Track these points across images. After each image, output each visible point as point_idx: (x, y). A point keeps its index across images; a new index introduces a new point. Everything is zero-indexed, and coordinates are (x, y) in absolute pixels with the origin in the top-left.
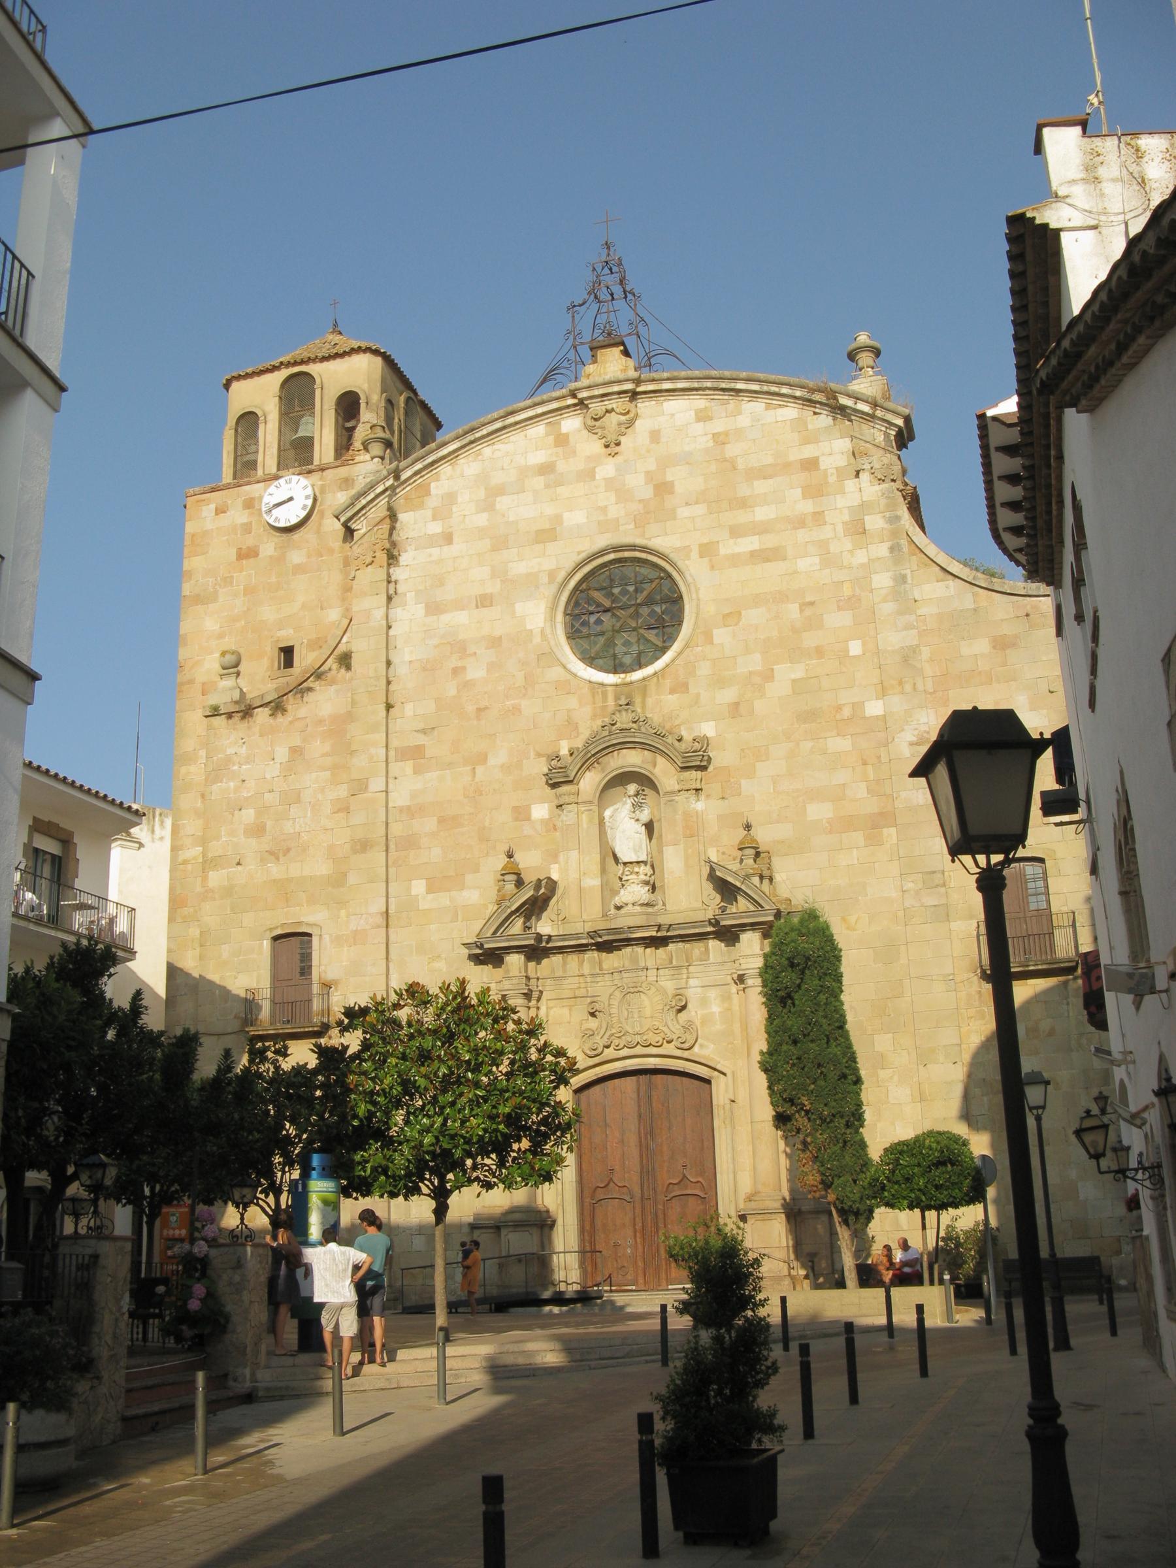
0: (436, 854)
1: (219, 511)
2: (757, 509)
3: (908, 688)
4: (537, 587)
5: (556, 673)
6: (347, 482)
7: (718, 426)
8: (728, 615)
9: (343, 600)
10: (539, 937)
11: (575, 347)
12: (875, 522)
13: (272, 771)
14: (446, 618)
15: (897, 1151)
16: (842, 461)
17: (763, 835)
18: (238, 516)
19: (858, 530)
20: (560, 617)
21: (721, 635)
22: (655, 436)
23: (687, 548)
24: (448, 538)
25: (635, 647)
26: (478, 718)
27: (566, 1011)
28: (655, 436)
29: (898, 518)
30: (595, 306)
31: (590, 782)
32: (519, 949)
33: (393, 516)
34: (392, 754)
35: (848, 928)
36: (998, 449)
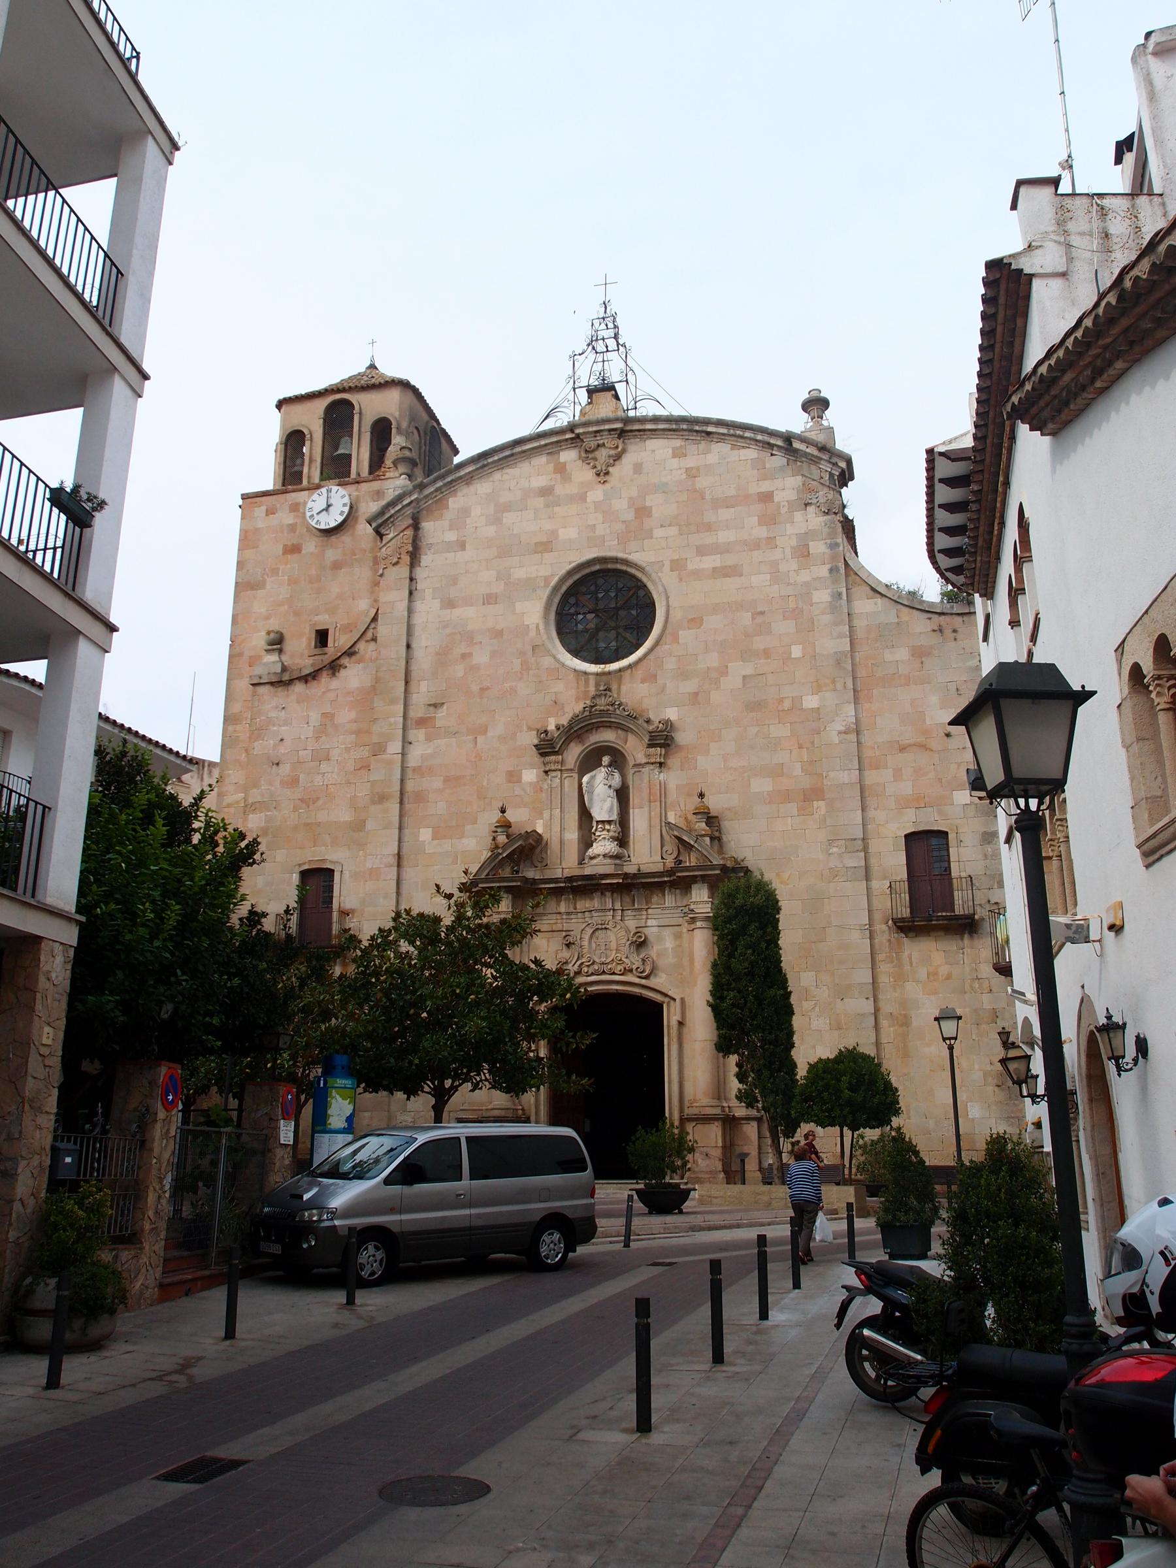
0: (442, 806)
1: (270, 512)
2: (720, 533)
3: (839, 686)
4: (534, 590)
5: (547, 662)
6: (379, 494)
7: (691, 462)
8: (692, 619)
9: (372, 593)
10: (526, 880)
11: (574, 389)
12: (818, 547)
13: (308, 732)
14: (457, 612)
15: (820, 1069)
16: (791, 495)
17: (714, 803)
19: (803, 553)
20: (552, 616)
21: (685, 635)
22: (638, 468)
23: (661, 564)
24: (462, 546)
25: (614, 643)
26: (481, 698)
28: (638, 468)
29: (837, 545)
30: (592, 356)
31: (574, 753)
32: (509, 890)
33: (416, 526)
34: (409, 722)
35: (781, 883)
36: (941, 481)
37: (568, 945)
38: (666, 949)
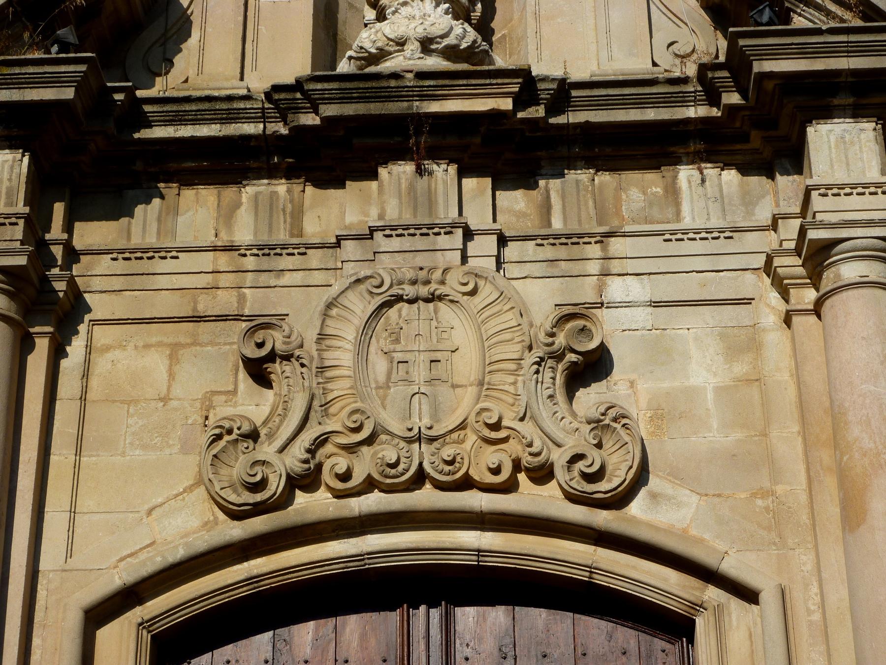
27: (156, 363)
37: (259, 371)
38: (692, 393)
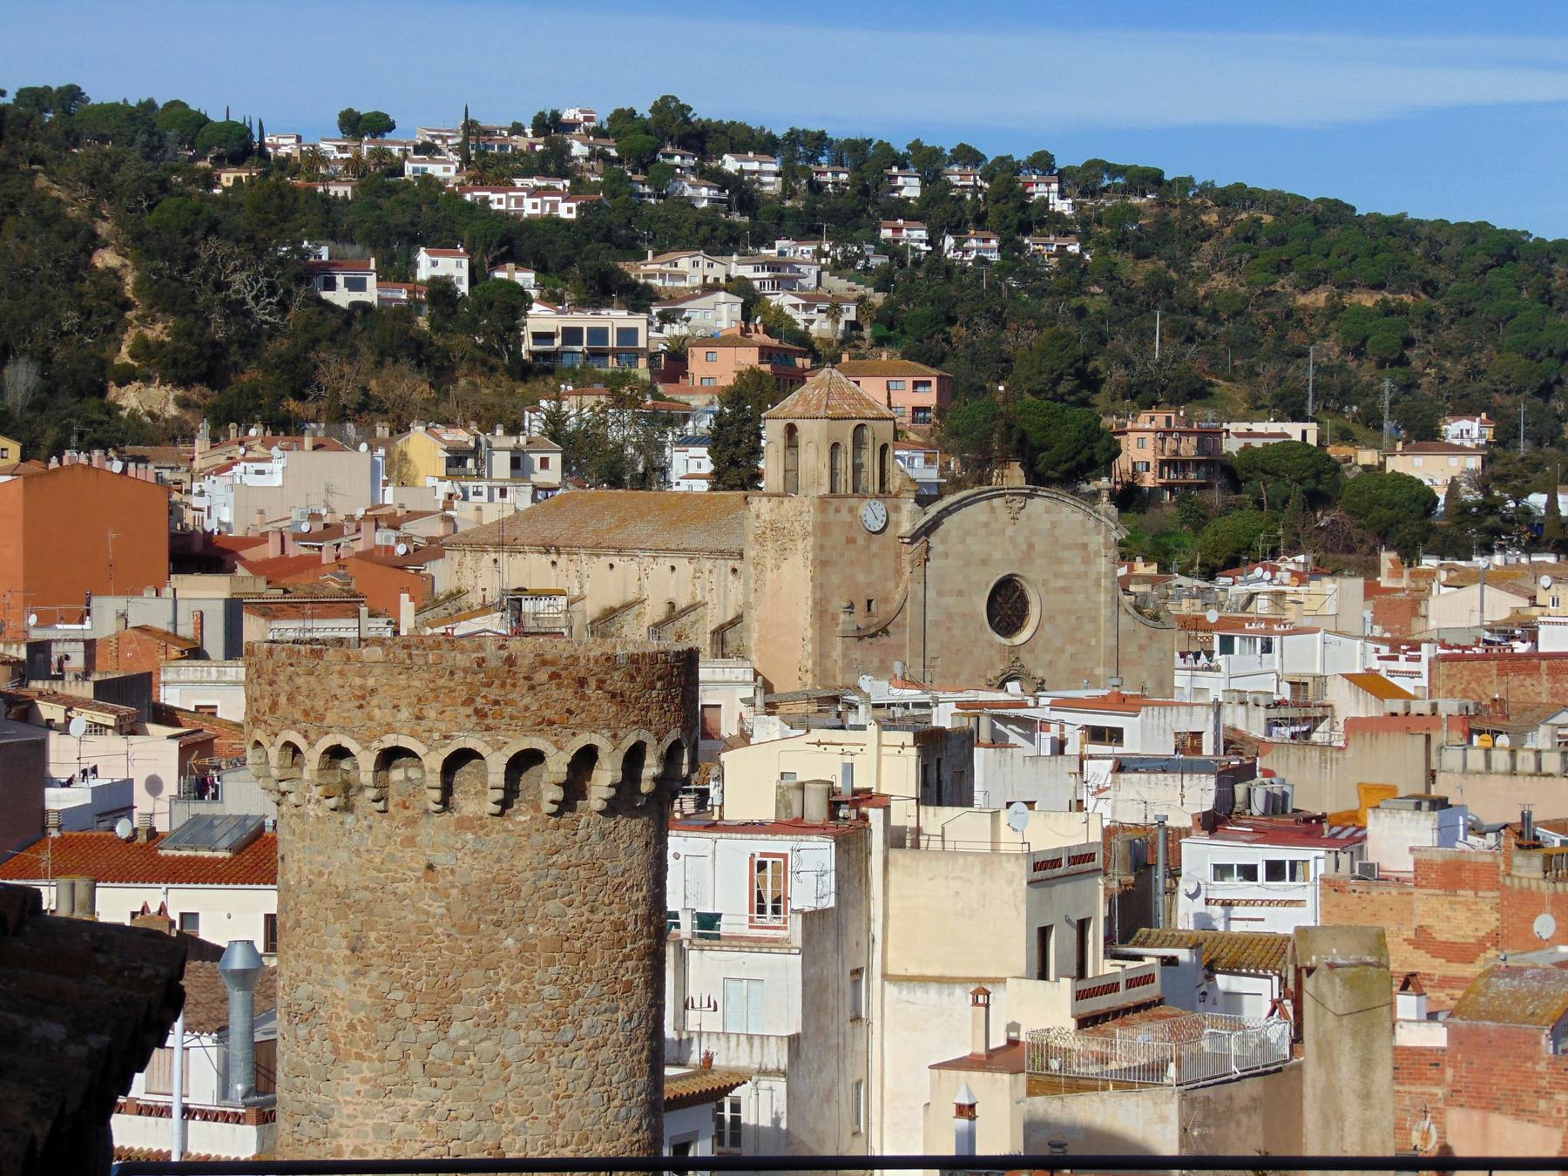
18: (845, 516)
22: (1029, 517)
28: (1029, 517)
